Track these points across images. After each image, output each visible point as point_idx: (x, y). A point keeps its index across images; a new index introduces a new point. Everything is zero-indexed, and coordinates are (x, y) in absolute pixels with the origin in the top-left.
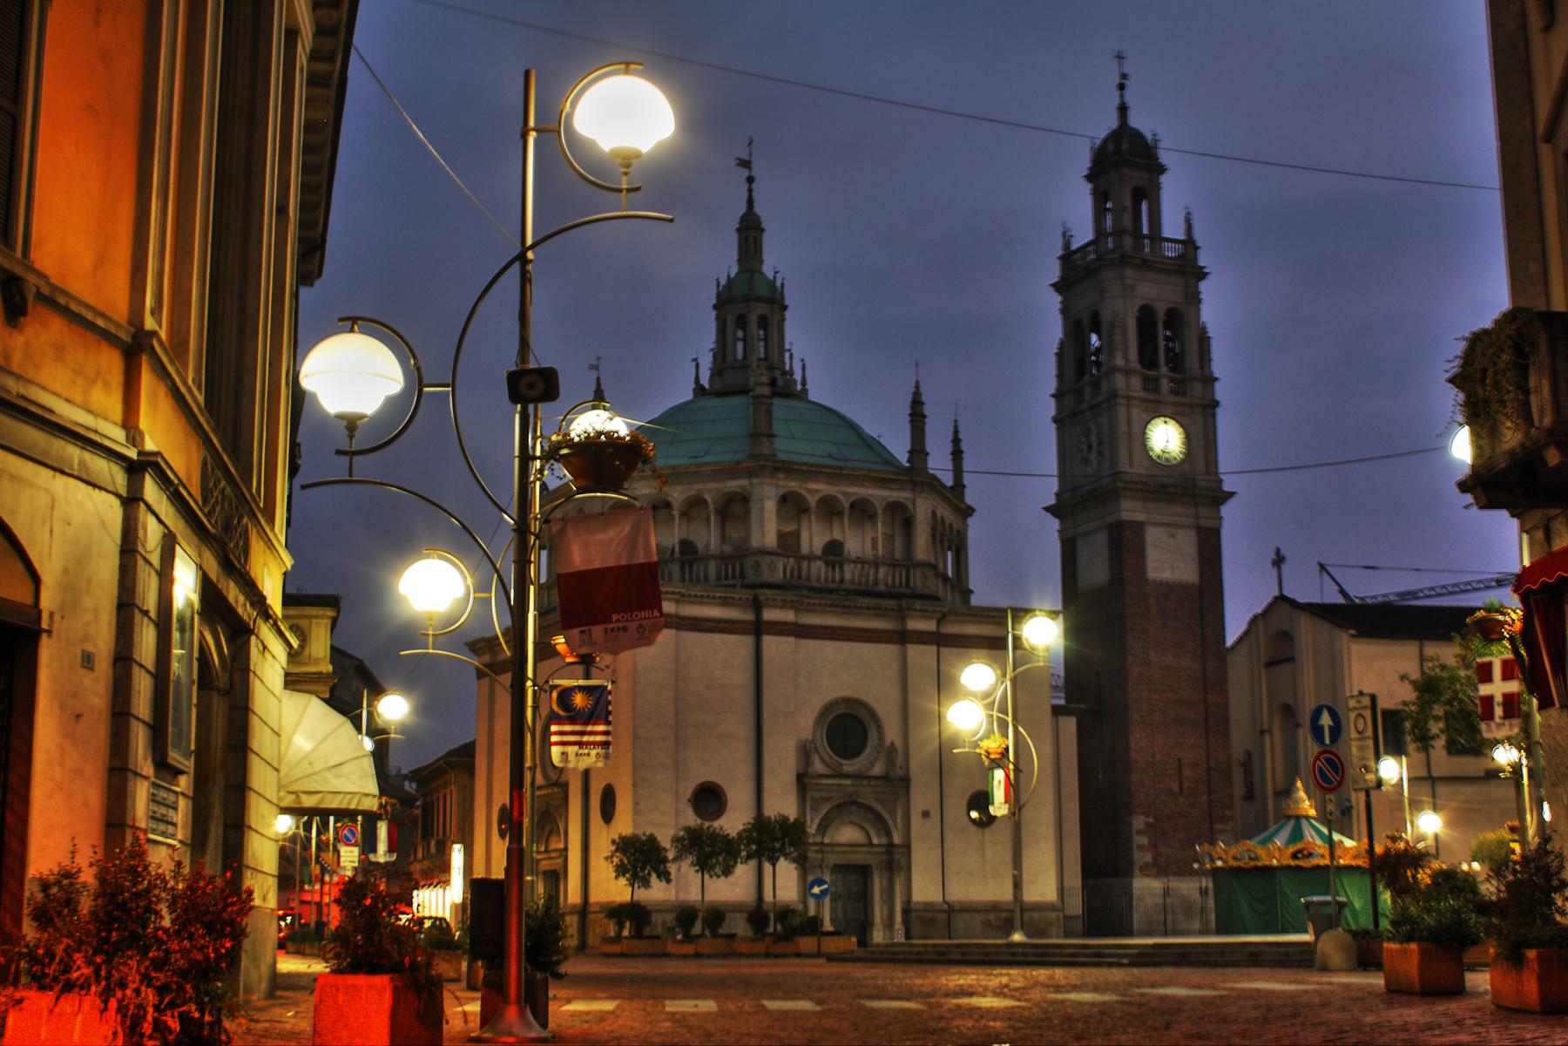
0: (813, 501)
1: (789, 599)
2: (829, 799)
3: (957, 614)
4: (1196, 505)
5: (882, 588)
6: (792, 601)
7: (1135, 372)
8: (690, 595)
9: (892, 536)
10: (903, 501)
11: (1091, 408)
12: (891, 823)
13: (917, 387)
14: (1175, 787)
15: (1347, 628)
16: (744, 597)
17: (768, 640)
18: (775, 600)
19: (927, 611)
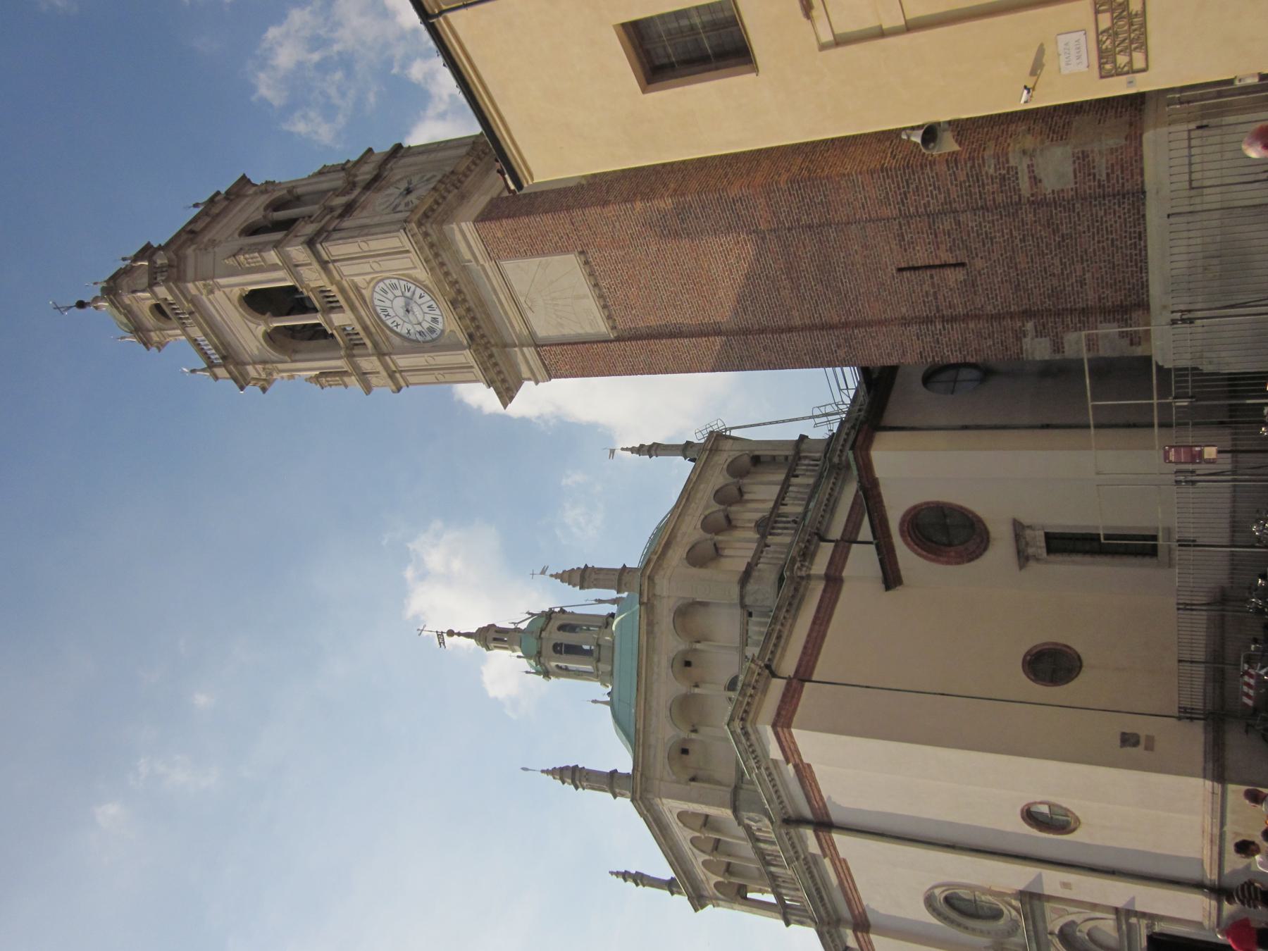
14: (960, 274)
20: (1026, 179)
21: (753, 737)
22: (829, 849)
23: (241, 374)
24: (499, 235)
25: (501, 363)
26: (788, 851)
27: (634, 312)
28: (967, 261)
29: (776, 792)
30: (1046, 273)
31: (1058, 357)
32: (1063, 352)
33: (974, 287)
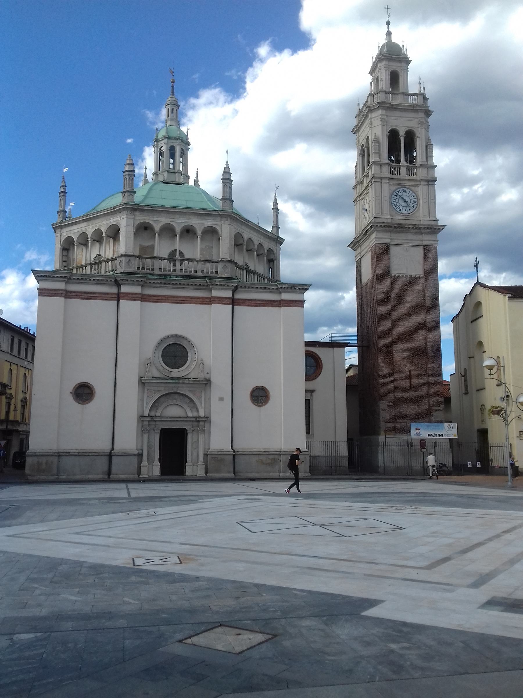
0: (157, 228)
1: (135, 279)
2: (159, 390)
3: (245, 287)
4: (422, 234)
5: (199, 274)
6: (138, 281)
11: (366, 188)
12: (198, 404)
13: (227, 164)
15: (506, 294)
16: (109, 279)
17: (122, 302)
20: (437, 409)
21: (298, 291)
23: (384, 106)
24: (432, 253)
25: (387, 228)
26: (220, 282)
29: (257, 288)
30: (407, 410)
31: (381, 411)
32: (382, 412)
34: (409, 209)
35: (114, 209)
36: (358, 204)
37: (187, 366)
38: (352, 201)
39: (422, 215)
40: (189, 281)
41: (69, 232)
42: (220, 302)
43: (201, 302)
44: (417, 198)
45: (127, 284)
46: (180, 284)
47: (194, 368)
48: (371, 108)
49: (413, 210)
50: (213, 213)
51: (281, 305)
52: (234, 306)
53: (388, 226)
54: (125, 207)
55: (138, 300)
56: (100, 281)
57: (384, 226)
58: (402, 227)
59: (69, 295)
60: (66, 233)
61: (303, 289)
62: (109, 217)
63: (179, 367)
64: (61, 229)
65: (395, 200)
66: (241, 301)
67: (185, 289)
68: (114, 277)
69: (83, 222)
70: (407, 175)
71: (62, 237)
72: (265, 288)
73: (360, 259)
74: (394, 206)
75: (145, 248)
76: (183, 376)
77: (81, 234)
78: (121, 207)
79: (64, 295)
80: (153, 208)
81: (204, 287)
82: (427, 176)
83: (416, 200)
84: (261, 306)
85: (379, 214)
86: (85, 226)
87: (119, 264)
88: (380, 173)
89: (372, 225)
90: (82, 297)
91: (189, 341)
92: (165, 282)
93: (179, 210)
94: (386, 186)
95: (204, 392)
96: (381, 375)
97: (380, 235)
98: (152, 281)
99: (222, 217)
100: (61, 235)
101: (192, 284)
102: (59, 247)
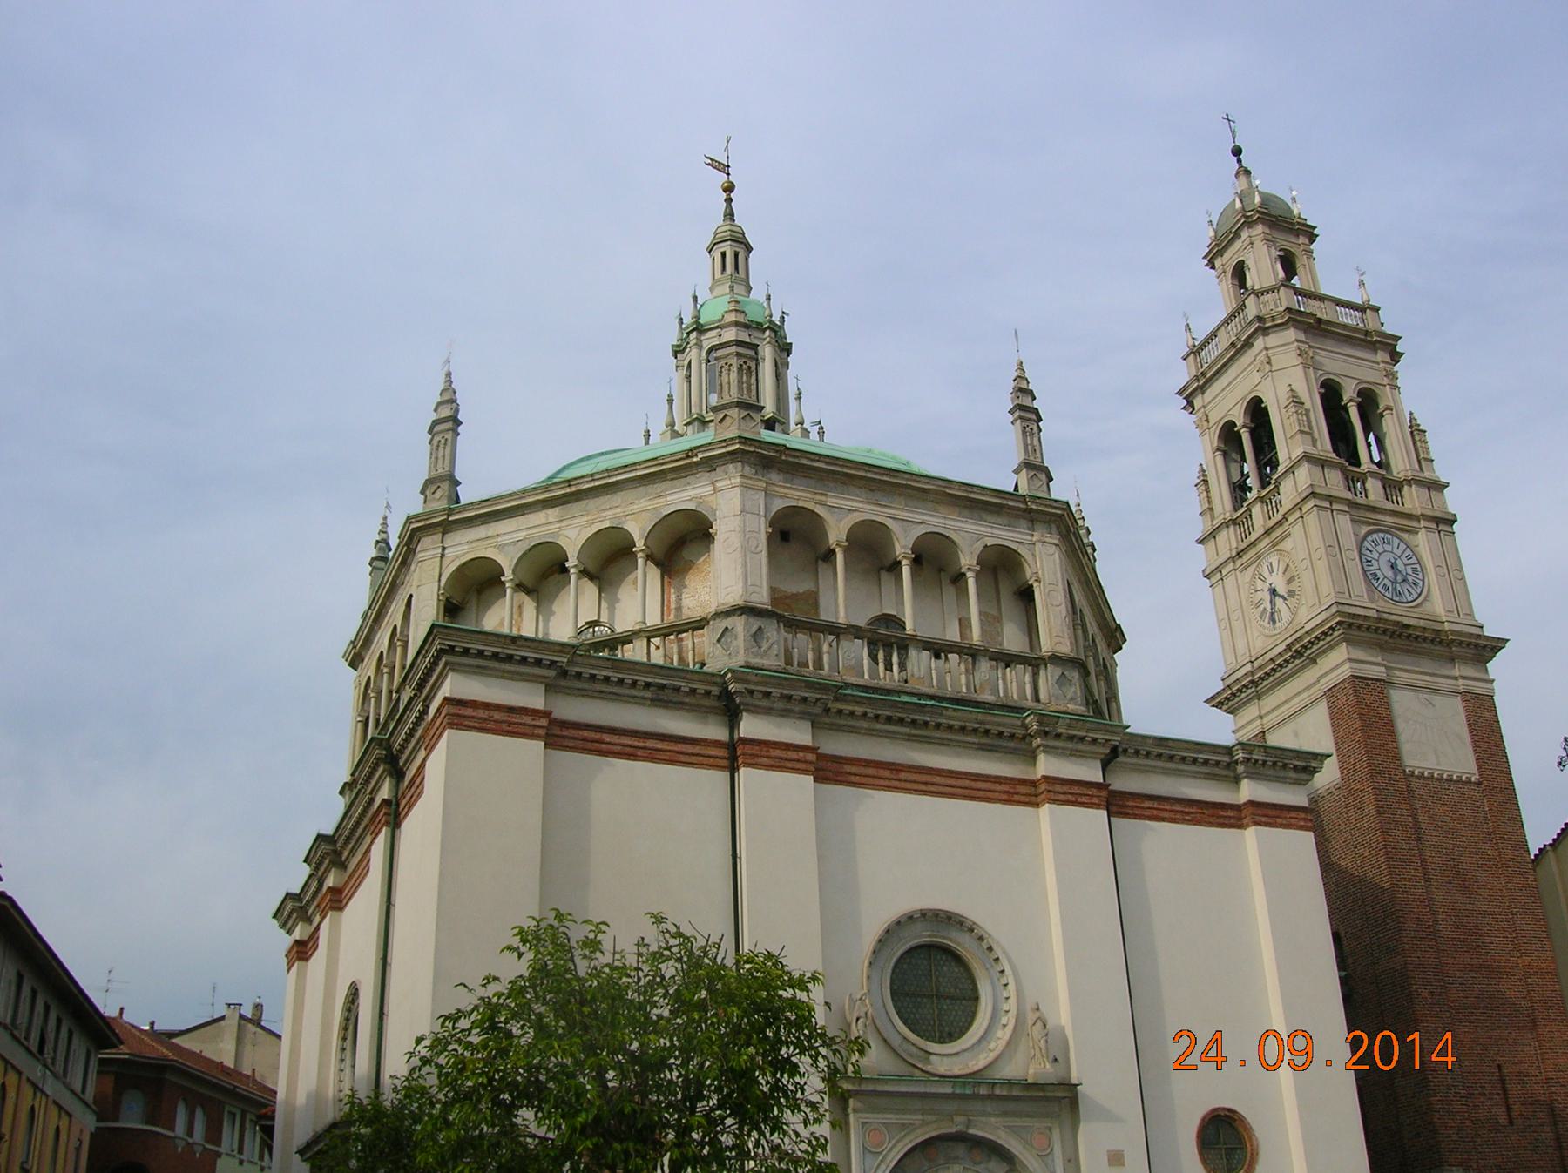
0: (837, 532)
1: (796, 694)
3: (1137, 752)
4: (1452, 660)
5: (988, 697)
6: (804, 700)
7: (1332, 464)
8: (579, 675)
9: (999, 619)
10: (1014, 546)
11: (1268, 532)
14: (1503, 1120)
16: (701, 688)
18: (767, 695)
19: (1082, 739)
21: (1292, 774)
22: (1065, 793)
23: (1299, 322)
24: (1487, 714)
25: (1375, 636)
26: (1070, 727)
27: (1430, 802)
28: (1515, 1127)
29: (1171, 758)
33: (1494, 1129)
34: (1409, 591)
35: (688, 457)
36: (1229, 581)
37: (981, 1032)
38: (1202, 576)
39: (1438, 606)
40: (970, 716)
41: (480, 543)
42: (1072, 798)
43: (1005, 797)
44: (1419, 563)
45: (764, 708)
46: (938, 726)
47: (1009, 1042)
48: (1264, 324)
49: (1416, 595)
50: (1010, 503)
51: (1246, 821)
52: (1112, 819)
53: (1376, 630)
54: (739, 448)
55: (806, 772)
56: (666, 691)
57: (1368, 628)
58: (1410, 635)
59: (557, 736)
60: (466, 547)
61: (1305, 769)
62: (658, 488)
63: (950, 1036)
64: (443, 534)
65: (1369, 563)
66: (1128, 801)
67: (948, 745)
68: (718, 680)
69: (544, 508)
70: (1387, 499)
71: (446, 561)
72: (1195, 760)
73: (1260, 736)
74: (1370, 577)
75: (787, 601)
76: (976, 1068)
77: (534, 546)
78: (723, 450)
79: (542, 732)
80: (827, 463)
81: (1012, 744)
82: (1431, 507)
83: (1419, 569)
84: (1189, 820)
85: (1340, 595)
86: (551, 520)
87: (719, 640)
88: (1324, 485)
89: (1338, 623)
90: (603, 746)
91: (981, 939)
92: (888, 713)
93: (907, 480)
94: (1344, 521)
95: (1058, 1130)
96: (1431, 1082)
97: (1359, 654)
98: (847, 707)
99: (1032, 521)
100: (442, 556)
101: (975, 730)
102: (436, 596)
